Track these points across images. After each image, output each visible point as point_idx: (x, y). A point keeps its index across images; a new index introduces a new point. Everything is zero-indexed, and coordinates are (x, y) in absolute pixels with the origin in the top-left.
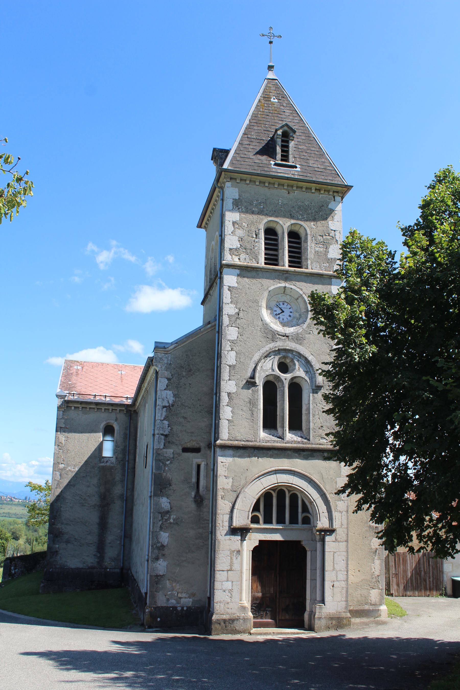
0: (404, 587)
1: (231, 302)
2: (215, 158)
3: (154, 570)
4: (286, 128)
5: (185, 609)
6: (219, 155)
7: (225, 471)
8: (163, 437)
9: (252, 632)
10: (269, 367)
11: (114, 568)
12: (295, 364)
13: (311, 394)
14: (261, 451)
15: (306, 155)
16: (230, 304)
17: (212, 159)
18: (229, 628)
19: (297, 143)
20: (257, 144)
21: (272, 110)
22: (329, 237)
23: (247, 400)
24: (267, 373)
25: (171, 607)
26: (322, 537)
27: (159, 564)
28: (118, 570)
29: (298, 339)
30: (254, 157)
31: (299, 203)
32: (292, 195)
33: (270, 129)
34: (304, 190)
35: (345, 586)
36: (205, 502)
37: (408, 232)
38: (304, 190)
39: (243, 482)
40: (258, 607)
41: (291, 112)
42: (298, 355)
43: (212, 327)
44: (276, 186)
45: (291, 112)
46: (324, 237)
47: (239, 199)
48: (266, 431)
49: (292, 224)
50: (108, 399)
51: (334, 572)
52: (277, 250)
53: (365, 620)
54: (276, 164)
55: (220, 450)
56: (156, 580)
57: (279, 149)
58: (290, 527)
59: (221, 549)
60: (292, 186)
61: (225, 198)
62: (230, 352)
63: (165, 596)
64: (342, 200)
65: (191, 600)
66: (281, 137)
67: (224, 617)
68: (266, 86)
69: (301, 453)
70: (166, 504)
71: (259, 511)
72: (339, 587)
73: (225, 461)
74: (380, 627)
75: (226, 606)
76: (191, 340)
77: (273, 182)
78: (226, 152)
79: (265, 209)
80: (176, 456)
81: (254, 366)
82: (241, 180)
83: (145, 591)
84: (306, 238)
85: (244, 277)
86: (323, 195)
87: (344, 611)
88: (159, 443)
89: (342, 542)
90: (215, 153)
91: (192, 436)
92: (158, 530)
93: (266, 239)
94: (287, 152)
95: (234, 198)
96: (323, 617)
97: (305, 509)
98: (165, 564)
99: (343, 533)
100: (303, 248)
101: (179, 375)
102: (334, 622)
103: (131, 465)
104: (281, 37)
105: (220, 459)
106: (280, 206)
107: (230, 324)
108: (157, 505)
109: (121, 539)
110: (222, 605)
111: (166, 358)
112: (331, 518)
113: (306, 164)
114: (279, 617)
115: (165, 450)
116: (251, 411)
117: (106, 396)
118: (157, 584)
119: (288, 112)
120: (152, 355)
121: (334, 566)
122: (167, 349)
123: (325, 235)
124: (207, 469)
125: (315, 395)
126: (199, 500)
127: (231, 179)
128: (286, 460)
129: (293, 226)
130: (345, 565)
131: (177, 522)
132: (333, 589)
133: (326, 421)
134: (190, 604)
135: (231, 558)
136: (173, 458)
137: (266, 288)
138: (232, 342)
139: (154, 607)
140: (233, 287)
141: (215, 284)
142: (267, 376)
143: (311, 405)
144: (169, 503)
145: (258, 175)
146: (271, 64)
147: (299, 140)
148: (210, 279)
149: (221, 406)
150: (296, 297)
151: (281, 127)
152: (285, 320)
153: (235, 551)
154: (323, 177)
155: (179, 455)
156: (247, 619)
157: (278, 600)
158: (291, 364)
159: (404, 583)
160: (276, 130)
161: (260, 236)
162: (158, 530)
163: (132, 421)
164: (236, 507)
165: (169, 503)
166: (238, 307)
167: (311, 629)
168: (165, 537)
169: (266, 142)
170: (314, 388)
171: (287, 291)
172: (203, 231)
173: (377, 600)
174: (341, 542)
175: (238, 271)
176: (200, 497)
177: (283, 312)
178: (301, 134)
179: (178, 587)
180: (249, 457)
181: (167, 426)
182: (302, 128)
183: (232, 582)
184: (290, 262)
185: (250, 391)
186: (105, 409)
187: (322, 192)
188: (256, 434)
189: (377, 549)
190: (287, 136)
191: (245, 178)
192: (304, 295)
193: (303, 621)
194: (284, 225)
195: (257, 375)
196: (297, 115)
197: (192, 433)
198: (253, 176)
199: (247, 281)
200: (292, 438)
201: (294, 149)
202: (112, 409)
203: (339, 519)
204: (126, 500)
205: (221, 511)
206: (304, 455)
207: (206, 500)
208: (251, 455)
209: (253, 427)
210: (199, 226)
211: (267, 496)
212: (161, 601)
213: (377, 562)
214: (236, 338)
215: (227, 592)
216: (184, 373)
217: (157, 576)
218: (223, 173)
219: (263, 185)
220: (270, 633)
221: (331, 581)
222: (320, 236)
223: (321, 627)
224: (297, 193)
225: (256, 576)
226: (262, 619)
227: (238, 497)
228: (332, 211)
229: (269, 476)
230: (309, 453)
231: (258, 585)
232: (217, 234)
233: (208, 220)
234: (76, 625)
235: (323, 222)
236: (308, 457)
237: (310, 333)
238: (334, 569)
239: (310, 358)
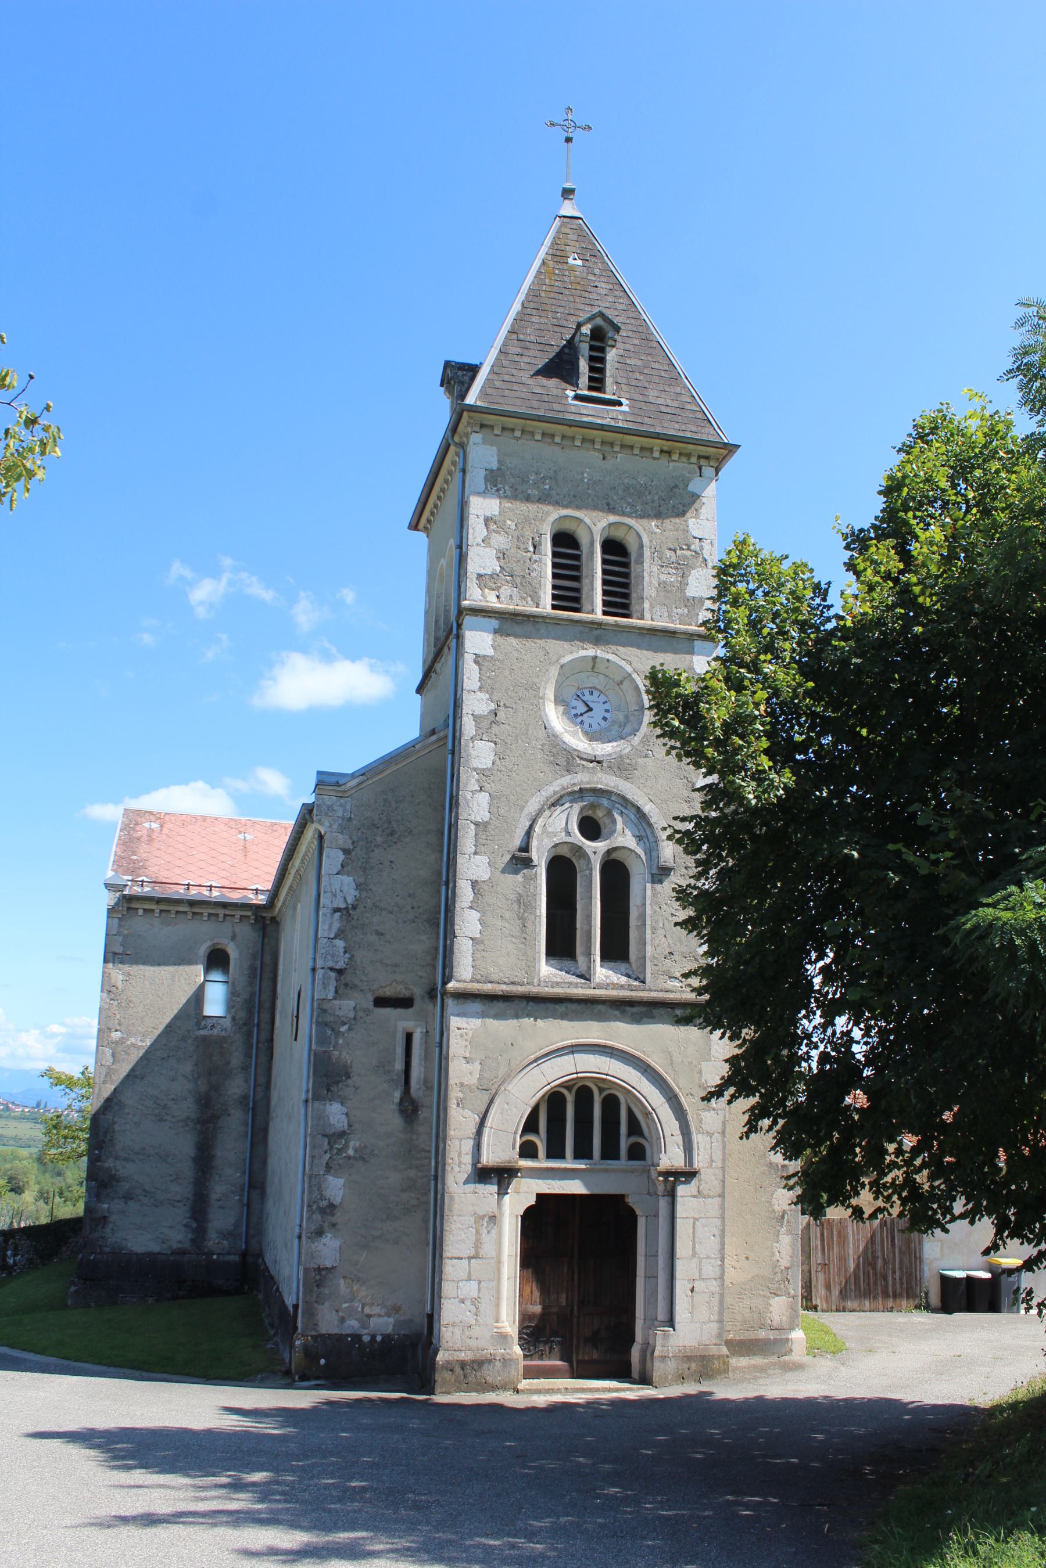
1: (481, 688)
2: (449, 383)
3: (313, 1257)
4: (599, 321)
5: (379, 1338)
6: (457, 376)
7: (466, 1046)
8: (333, 974)
9: (520, 1387)
10: (560, 828)
11: (228, 1254)
12: (614, 822)
13: (649, 885)
14: (542, 1006)
15: (641, 378)
16: (479, 693)
17: (442, 385)
18: (471, 1379)
19: (622, 352)
20: (539, 354)
21: (571, 283)
22: (689, 553)
23: (514, 897)
24: (556, 840)
25: (348, 1335)
26: (669, 1188)
27: (325, 1245)
28: (236, 1258)
29: (621, 766)
30: (531, 381)
31: (626, 481)
32: (610, 463)
33: (565, 323)
34: (636, 451)
35: (717, 1289)
36: (423, 1114)
37: (858, 541)
38: (636, 451)
39: (503, 1071)
40: (536, 1334)
41: (611, 286)
42: (621, 801)
43: (439, 740)
44: (578, 443)
45: (611, 286)
46: (679, 552)
47: (499, 469)
48: (552, 962)
49: (610, 525)
50: (215, 893)
51: (696, 1260)
52: (577, 579)
53: (758, 1360)
54: (577, 397)
55: (455, 1002)
56: (317, 1278)
57: (583, 366)
59: (455, 1212)
60: (612, 444)
61: (469, 468)
62: (477, 795)
63: (337, 1311)
64: (717, 474)
65: (391, 1320)
66: (588, 339)
68: (558, 232)
69: (628, 1009)
70: (340, 1117)
71: (536, 1131)
73: (465, 1025)
74: (789, 1375)
76: (394, 768)
77: (571, 435)
78: (473, 370)
79: (553, 492)
80: (361, 1014)
81: (528, 824)
82: (504, 429)
83: (295, 1302)
84: (641, 555)
85: (508, 635)
86: (677, 464)
88: (325, 988)
89: (713, 1197)
90: (449, 371)
91: (395, 972)
92: (322, 1173)
93: (555, 554)
94: (602, 371)
95: (489, 467)
97: (635, 1128)
100: (633, 575)
101: (367, 843)
102: (693, 1366)
103: (264, 1035)
104: (590, 128)
105: (455, 1022)
106: (586, 486)
107: (477, 734)
108: (319, 1119)
109: (243, 1190)
110: (457, 1331)
111: (341, 805)
112: (688, 1148)
113: (641, 398)
114: (577, 1355)
115: (337, 1002)
116: (522, 918)
117: (211, 886)
118: (318, 1286)
119: (603, 287)
120: (310, 799)
122: (343, 787)
123: (681, 549)
124: (426, 1042)
125: (658, 886)
126: (410, 1107)
127: (482, 426)
128: (595, 1023)
129: (612, 528)
130: (717, 1247)
131: (362, 1156)
132: (692, 1297)
133: (680, 941)
134: (389, 1330)
135: (478, 1232)
136: (355, 1019)
137: (554, 659)
138: (482, 772)
139: (312, 1336)
140: (484, 657)
141: (446, 649)
142: (556, 846)
143: (648, 907)
144: (347, 1114)
145: (540, 419)
146: (568, 185)
147: (627, 347)
148: (437, 639)
149: (457, 908)
150: (618, 678)
151: (590, 319)
152: (595, 727)
153: (485, 1216)
154: (677, 426)
155: (368, 1012)
156: (511, 1360)
157: (575, 1320)
158: (607, 820)
159: (840, 1284)
160: (579, 326)
161: (543, 547)
162: (322, 1173)
163: (266, 940)
164: (489, 1122)
165: (347, 1114)
166: (495, 698)
167: (645, 1380)
168: (335, 1187)
169: (557, 350)
170: (655, 871)
171: (600, 667)
172: (421, 537)
173: (784, 1318)
174: (709, 1197)
175: (495, 623)
176: (413, 1102)
177: (590, 710)
178: (630, 334)
179: (363, 1294)
180: (517, 1016)
181: (342, 951)
182: (633, 321)
183: (480, 1282)
184: (605, 603)
185: (519, 878)
186: (210, 915)
187: (675, 457)
188: (531, 968)
190: (600, 339)
191: (511, 426)
192: (635, 676)
193: (629, 1364)
194: (594, 526)
195: (534, 843)
196: (622, 294)
197: (396, 966)
198: (528, 422)
199: (515, 644)
200: (607, 977)
201: (617, 365)
202: (225, 915)
203: (705, 1148)
204: (254, 1109)
206: (632, 1014)
207: (424, 1110)
209: (525, 954)
210: (414, 526)
211: (554, 1100)
212: (328, 1322)
213: (785, 1240)
214: (490, 765)
215: (468, 1303)
216: (379, 839)
217: (319, 1270)
218: (465, 414)
219: (550, 440)
220: (559, 1389)
221: (689, 1280)
222: (670, 549)
223: (666, 1378)
224: (621, 460)
227: (491, 1102)
228: (695, 497)
230: (644, 1009)
231: (534, 1288)
232: (452, 543)
233: (432, 514)
234: (145, 1374)
235: (677, 520)
236: (642, 1018)
237: (646, 756)
238: (694, 1254)
239: (647, 808)
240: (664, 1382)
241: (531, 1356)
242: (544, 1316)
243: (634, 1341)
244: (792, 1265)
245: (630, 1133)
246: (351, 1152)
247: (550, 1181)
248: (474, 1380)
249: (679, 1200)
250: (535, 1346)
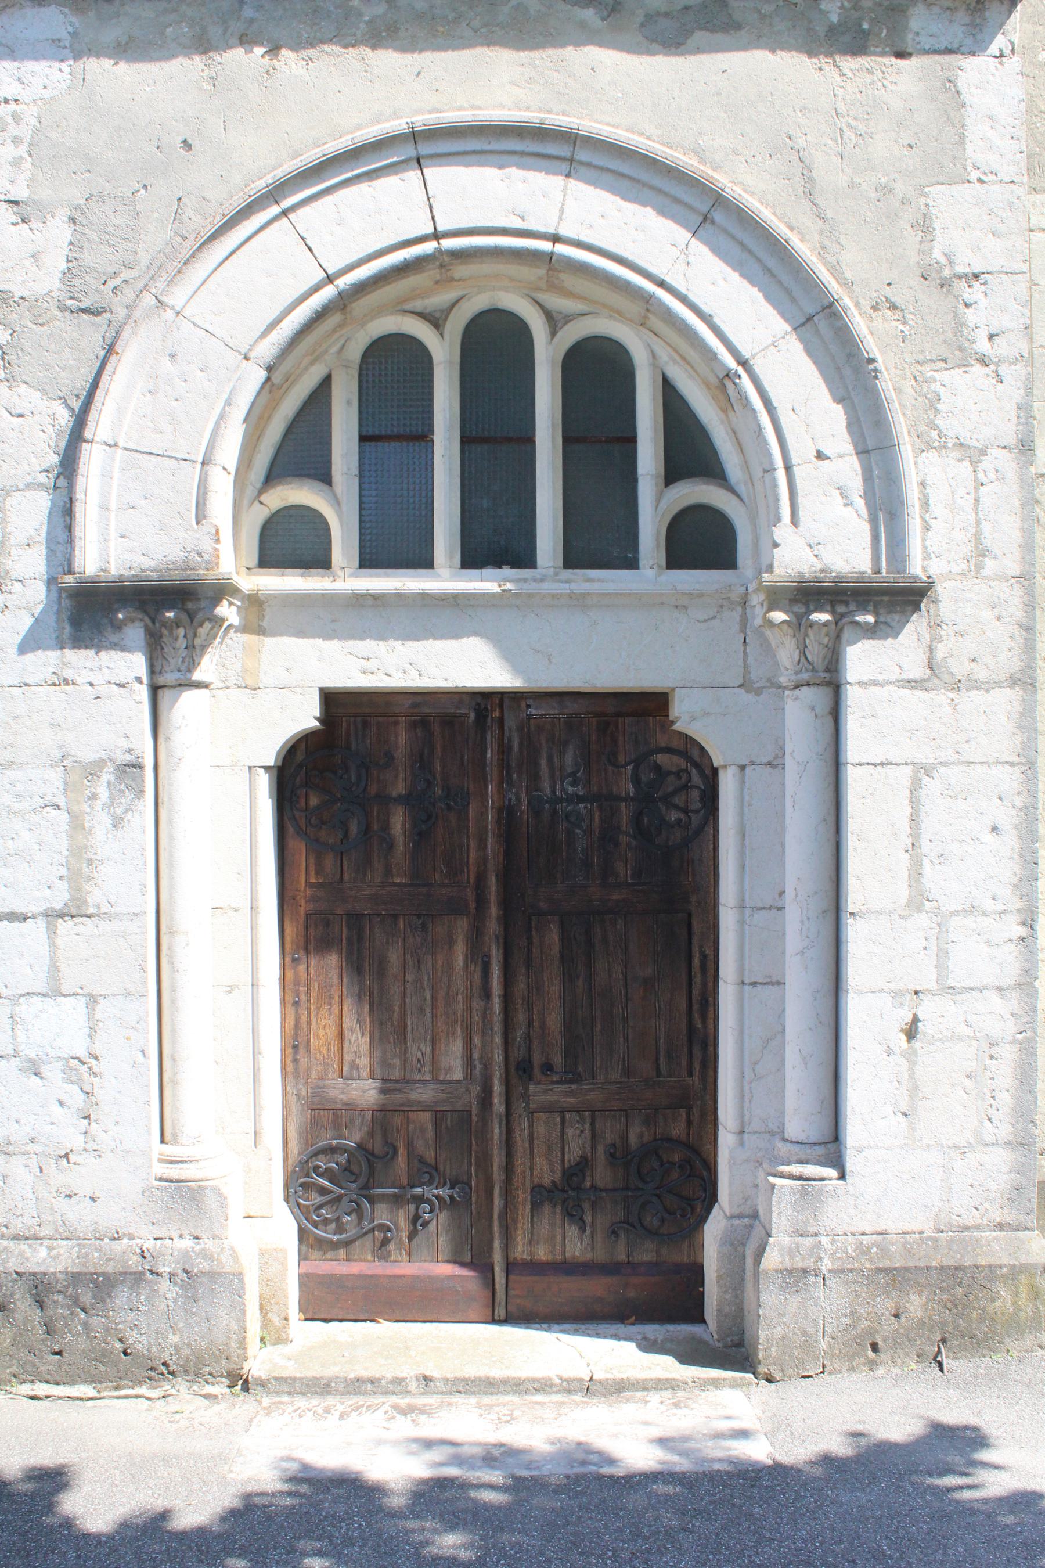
7: (17, 163)
18: (74, 1338)
26: (816, 652)
35: (1011, 1027)
40: (356, 1176)
51: (922, 920)
58: (562, 588)
67: (39, 1258)
71: (321, 474)
72: (960, 1039)
75: (58, 1177)
87: (997, 1216)
89: (986, 686)
96: (826, 1265)
97: (690, 452)
99: (988, 614)
102: (915, 1305)
112: (885, 502)
114: (507, 1248)
121: (916, 875)
130: (1010, 871)
132: (911, 1057)
135: (77, 823)
153: (100, 763)
156: (213, 1276)
157: (497, 1131)
164: (102, 424)
174: (975, 685)
183: (93, 1000)
208: (215, 32)
215: (53, 1072)
220: (398, 1381)
221: (897, 994)
223: (808, 1344)
225: (333, 960)
226: (385, 1258)
229: (364, 187)
238: (919, 899)
240: (806, 1364)
241: (347, 1244)
242: (384, 1119)
243: (711, 1198)
245: (672, 475)
248: (83, 1344)
249: (853, 697)
250: (359, 1211)
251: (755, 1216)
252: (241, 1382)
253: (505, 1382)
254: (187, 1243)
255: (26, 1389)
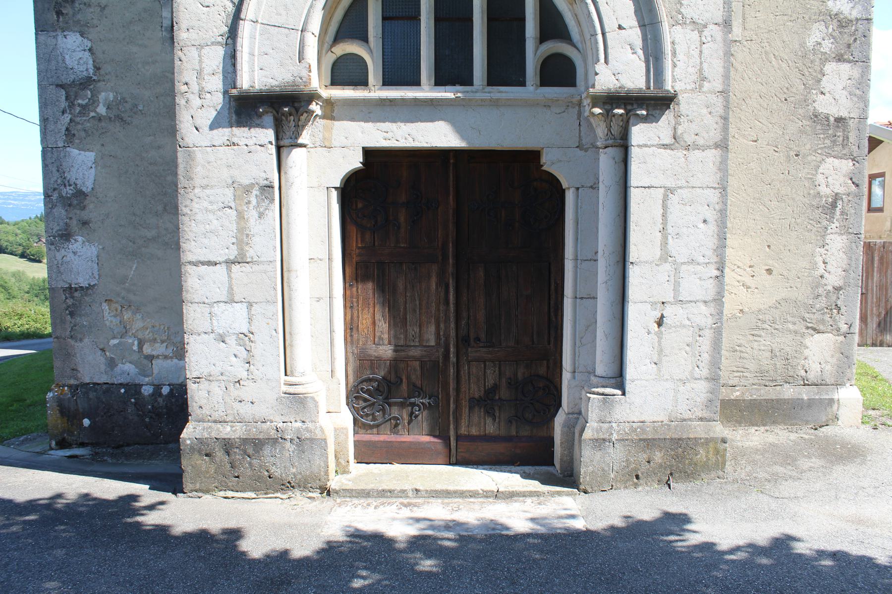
0: (879, 325)
5: (165, 390)
9: (334, 483)
18: (244, 470)
26: (616, 130)
27: (75, 253)
35: (710, 321)
51: (667, 266)
53: (780, 435)
56: (70, 302)
58: (486, 96)
59: (198, 181)
63: (103, 350)
67: (226, 431)
70: (80, 55)
72: (684, 326)
74: (841, 473)
75: (235, 392)
87: (700, 414)
89: (703, 148)
92: (61, 144)
96: (615, 437)
98: (92, 251)
99: (705, 111)
102: (658, 457)
110: (217, 390)
112: (653, 52)
114: (457, 428)
121: (664, 243)
130: (711, 242)
132: (659, 335)
135: (241, 216)
144: (90, 50)
153: (252, 185)
156: (312, 440)
159: (879, 316)
162: (61, 144)
165: (90, 50)
167: (568, 478)
168: (83, 165)
173: (828, 368)
174: (697, 147)
179: (138, 324)
183: (250, 305)
189: (837, 197)
203: (688, 55)
205: (193, 35)
212: (91, 366)
213: (837, 242)
215: (231, 340)
220: (403, 491)
221: (653, 304)
226: (397, 433)
231: (378, 316)
238: (666, 256)
240: (603, 485)
241: (378, 426)
242: (396, 364)
243: (559, 405)
244: (847, 284)
245: (544, 37)
246: (102, 110)
247: (387, 125)
249: (635, 153)
250: (383, 410)
251: (580, 413)
252: (326, 491)
253: (455, 492)
254: (299, 424)
255: (222, 493)
